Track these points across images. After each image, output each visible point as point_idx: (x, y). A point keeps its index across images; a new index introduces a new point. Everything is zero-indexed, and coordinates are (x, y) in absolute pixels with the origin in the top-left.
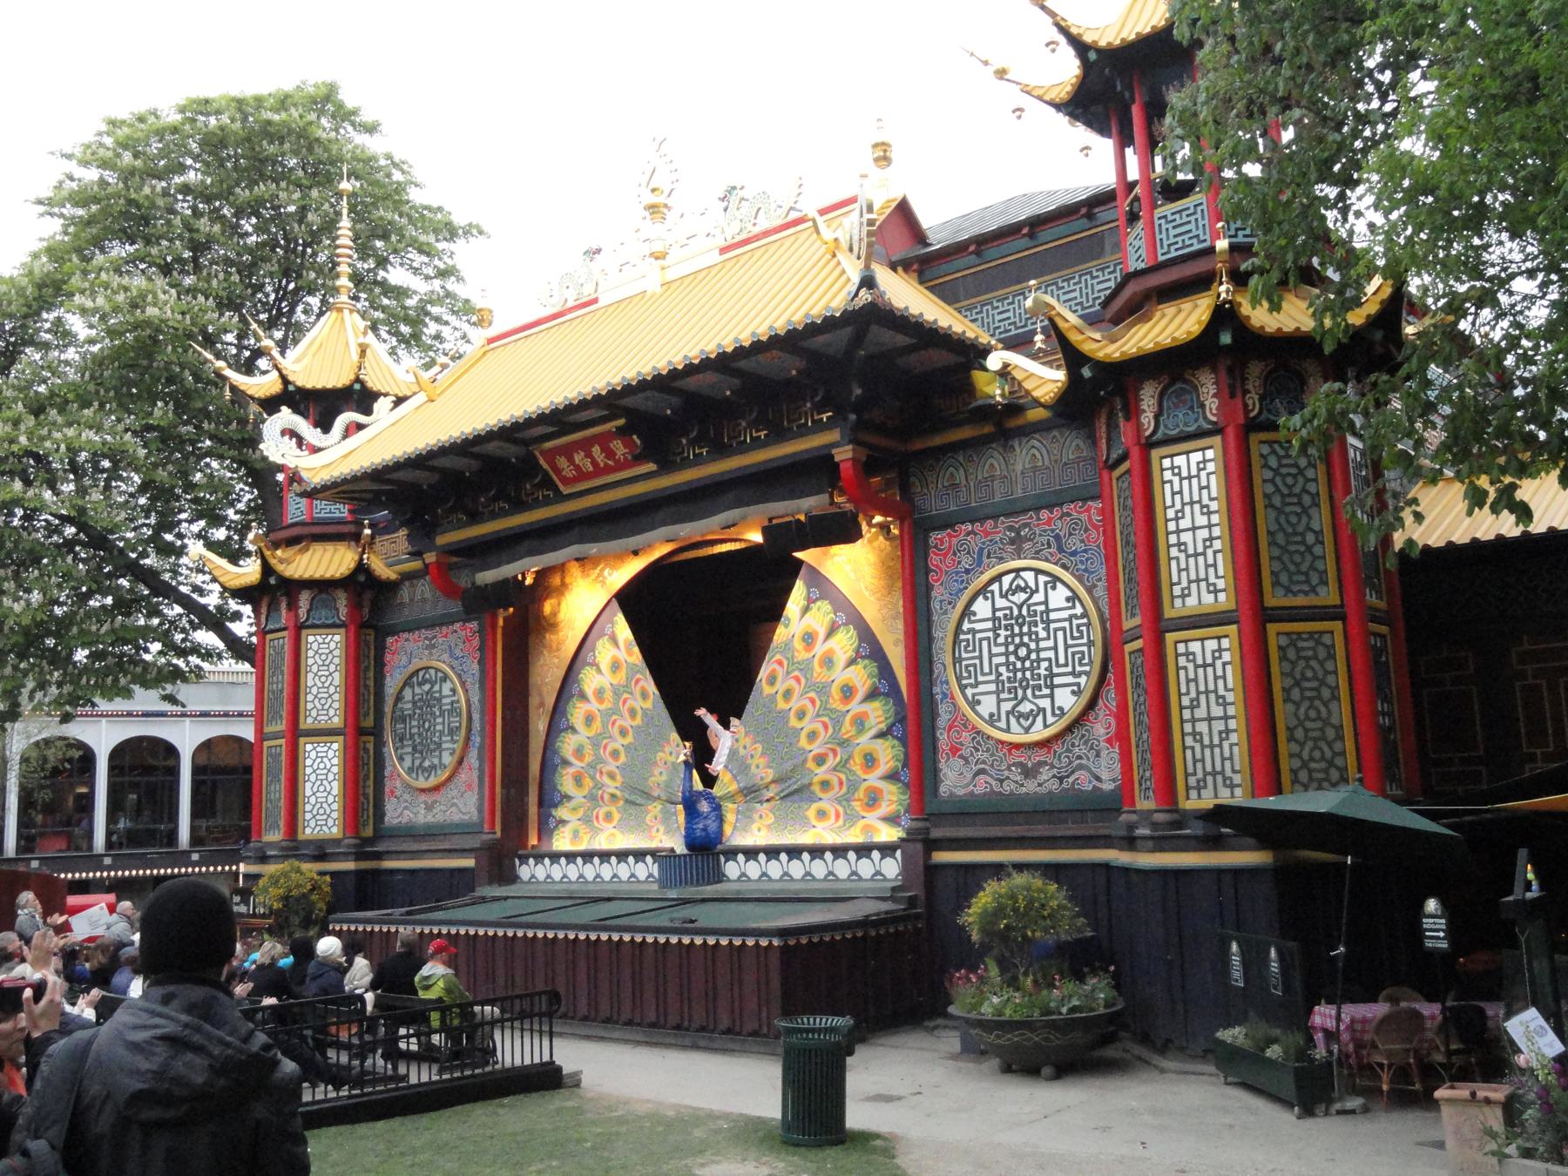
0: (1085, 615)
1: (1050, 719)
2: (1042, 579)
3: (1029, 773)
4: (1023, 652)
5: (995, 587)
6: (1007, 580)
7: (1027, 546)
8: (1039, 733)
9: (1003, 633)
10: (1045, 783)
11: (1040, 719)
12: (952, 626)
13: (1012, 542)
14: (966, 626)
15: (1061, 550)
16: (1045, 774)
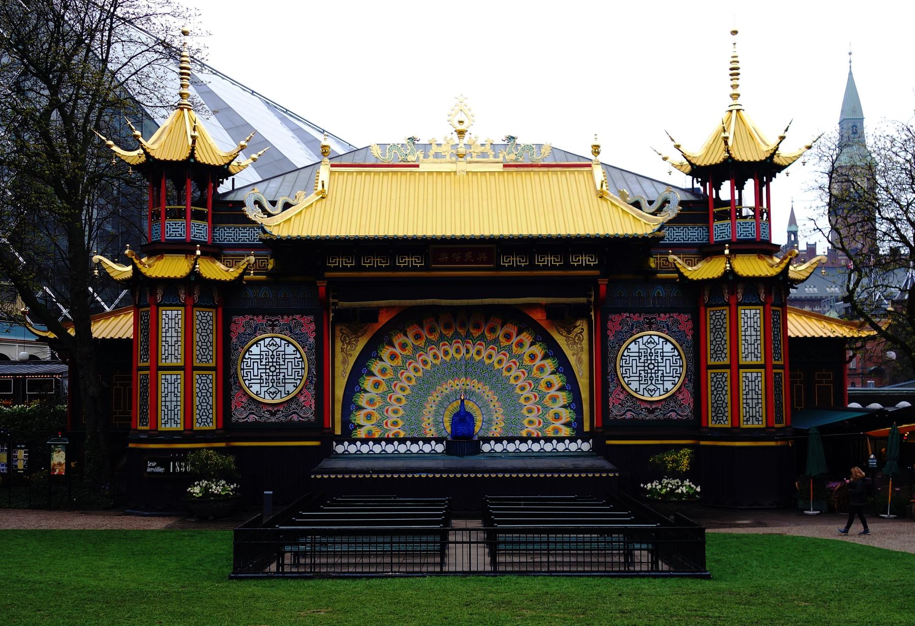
0: (301, 357)
1: (283, 395)
2: (283, 342)
3: (273, 414)
4: (273, 369)
5: (262, 342)
6: (267, 341)
7: (276, 328)
8: (278, 400)
9: (264, 361)
10: (280, 417)
11: (279, 395)
12: (241, 355)
13: (270, 325)
14: (247, 356)
15: (291, 332)
16: (279, 414)
